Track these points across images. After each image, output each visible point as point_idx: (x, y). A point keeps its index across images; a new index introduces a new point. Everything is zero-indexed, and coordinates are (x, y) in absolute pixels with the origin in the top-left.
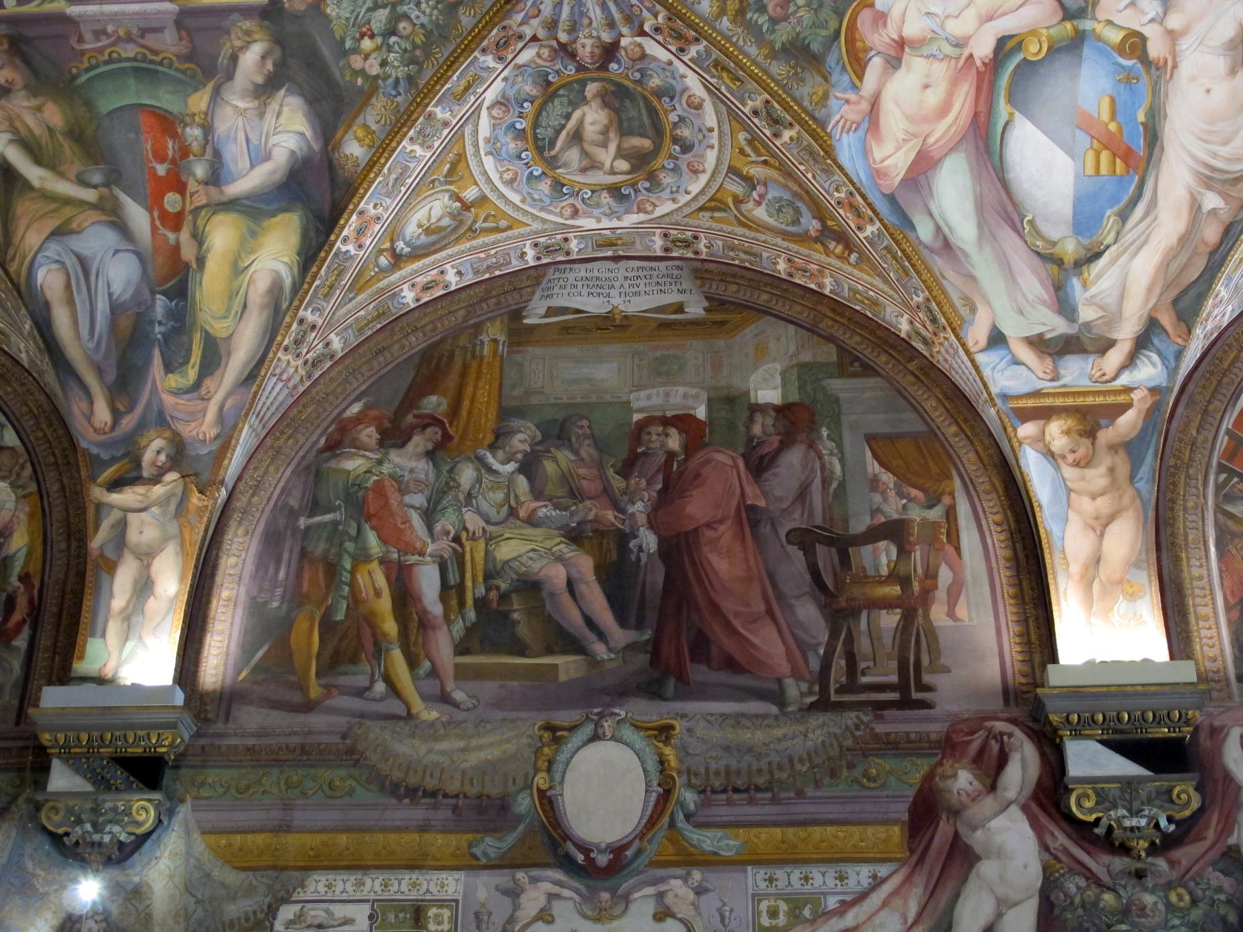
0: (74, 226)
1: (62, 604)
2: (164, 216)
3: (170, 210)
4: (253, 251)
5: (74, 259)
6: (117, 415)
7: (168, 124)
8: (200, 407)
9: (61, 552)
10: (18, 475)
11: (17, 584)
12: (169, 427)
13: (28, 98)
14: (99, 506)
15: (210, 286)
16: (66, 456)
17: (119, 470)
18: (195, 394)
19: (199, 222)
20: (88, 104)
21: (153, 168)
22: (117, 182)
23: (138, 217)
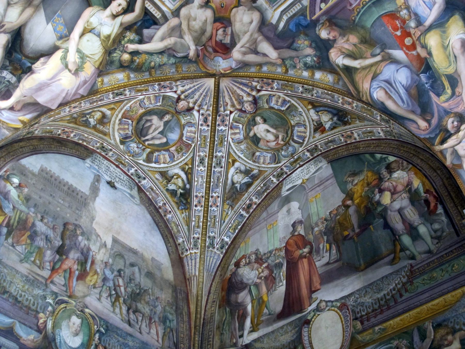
0: (378, 72)
1: (448, 191)
2: (408, 48)
3: (409, 44)
4: (447, 38)
5: (384, 83)
6: (429, 122)
7: (393, 16)
8: (460, 99)
9: (435, 176)
10: (403, 166)
11: (425, 195)
12: (452, 113)
13: (342, 39)
14: (441, 152)
15: (439, 61)
16: (416, 151)
17: (441, 137)
18: (455, 97)
19: (422, 41)
20: (363, 27)
21: (396, 35)
22: (385, 48)
23: (399, 54)
